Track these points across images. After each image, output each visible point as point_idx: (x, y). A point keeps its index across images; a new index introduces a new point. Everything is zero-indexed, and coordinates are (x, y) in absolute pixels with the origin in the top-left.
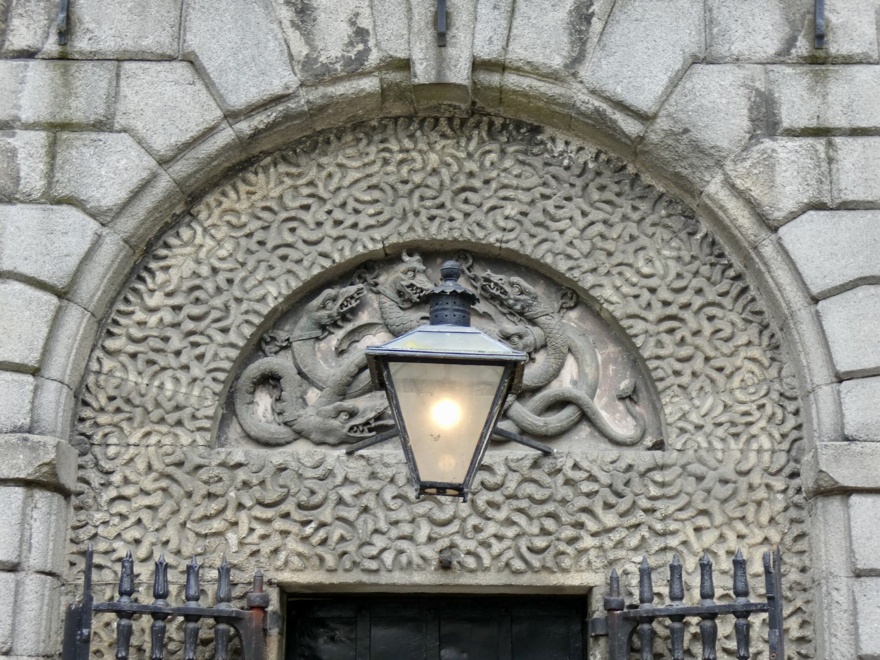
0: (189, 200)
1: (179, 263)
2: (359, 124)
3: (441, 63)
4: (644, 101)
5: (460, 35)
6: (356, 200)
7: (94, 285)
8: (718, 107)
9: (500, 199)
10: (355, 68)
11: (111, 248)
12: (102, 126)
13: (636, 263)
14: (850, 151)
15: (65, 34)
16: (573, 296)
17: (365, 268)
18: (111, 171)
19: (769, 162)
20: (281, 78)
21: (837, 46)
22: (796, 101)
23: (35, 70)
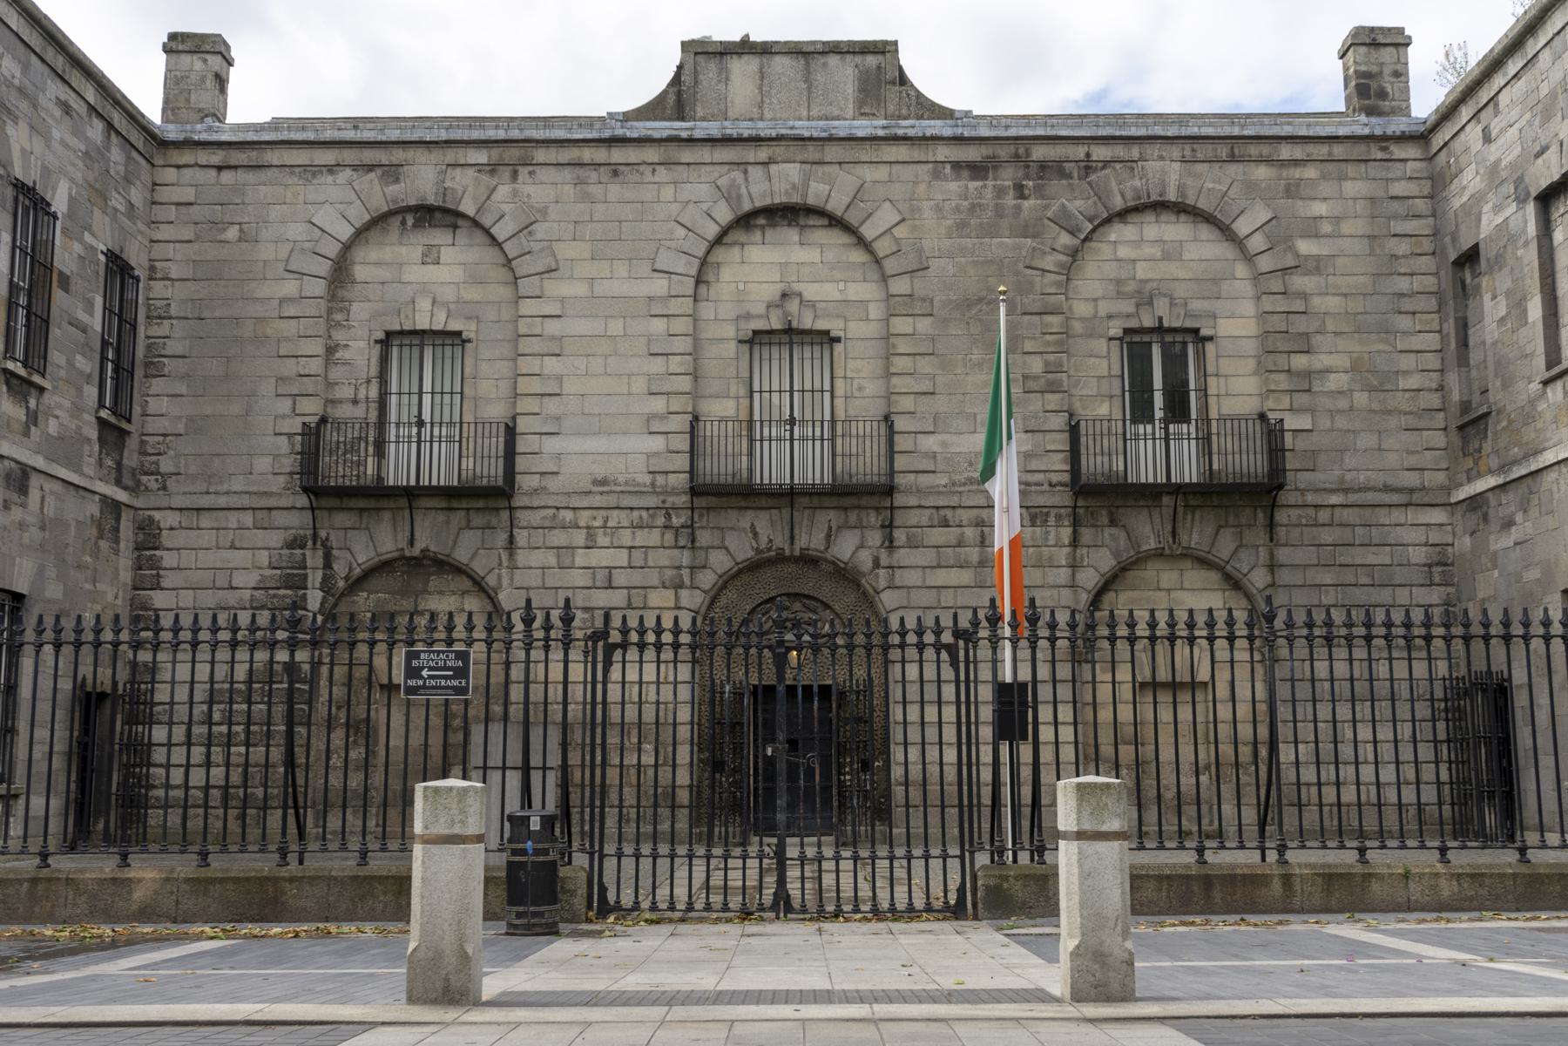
0: (724, 586)
1: (723, 600)
2: (771, 562)
3: (792, 550)
4: (845, 559)
5: (797, 541)
6: (768, 584)
7: (703, 610)
8: (865, 559)
9: (809, 583)
10: (769, 550)
11: (708, 600)
12: (704, 567)
13: (844, 602)
14: (898, 572)
15: (693, 542)
16: (827, 606)
17: (771, 600)
18: (707, 579)
19: (877, 576)
20: (751, 554)
21: (896, 543)
22: (884, 561)
23: (686, 553)
